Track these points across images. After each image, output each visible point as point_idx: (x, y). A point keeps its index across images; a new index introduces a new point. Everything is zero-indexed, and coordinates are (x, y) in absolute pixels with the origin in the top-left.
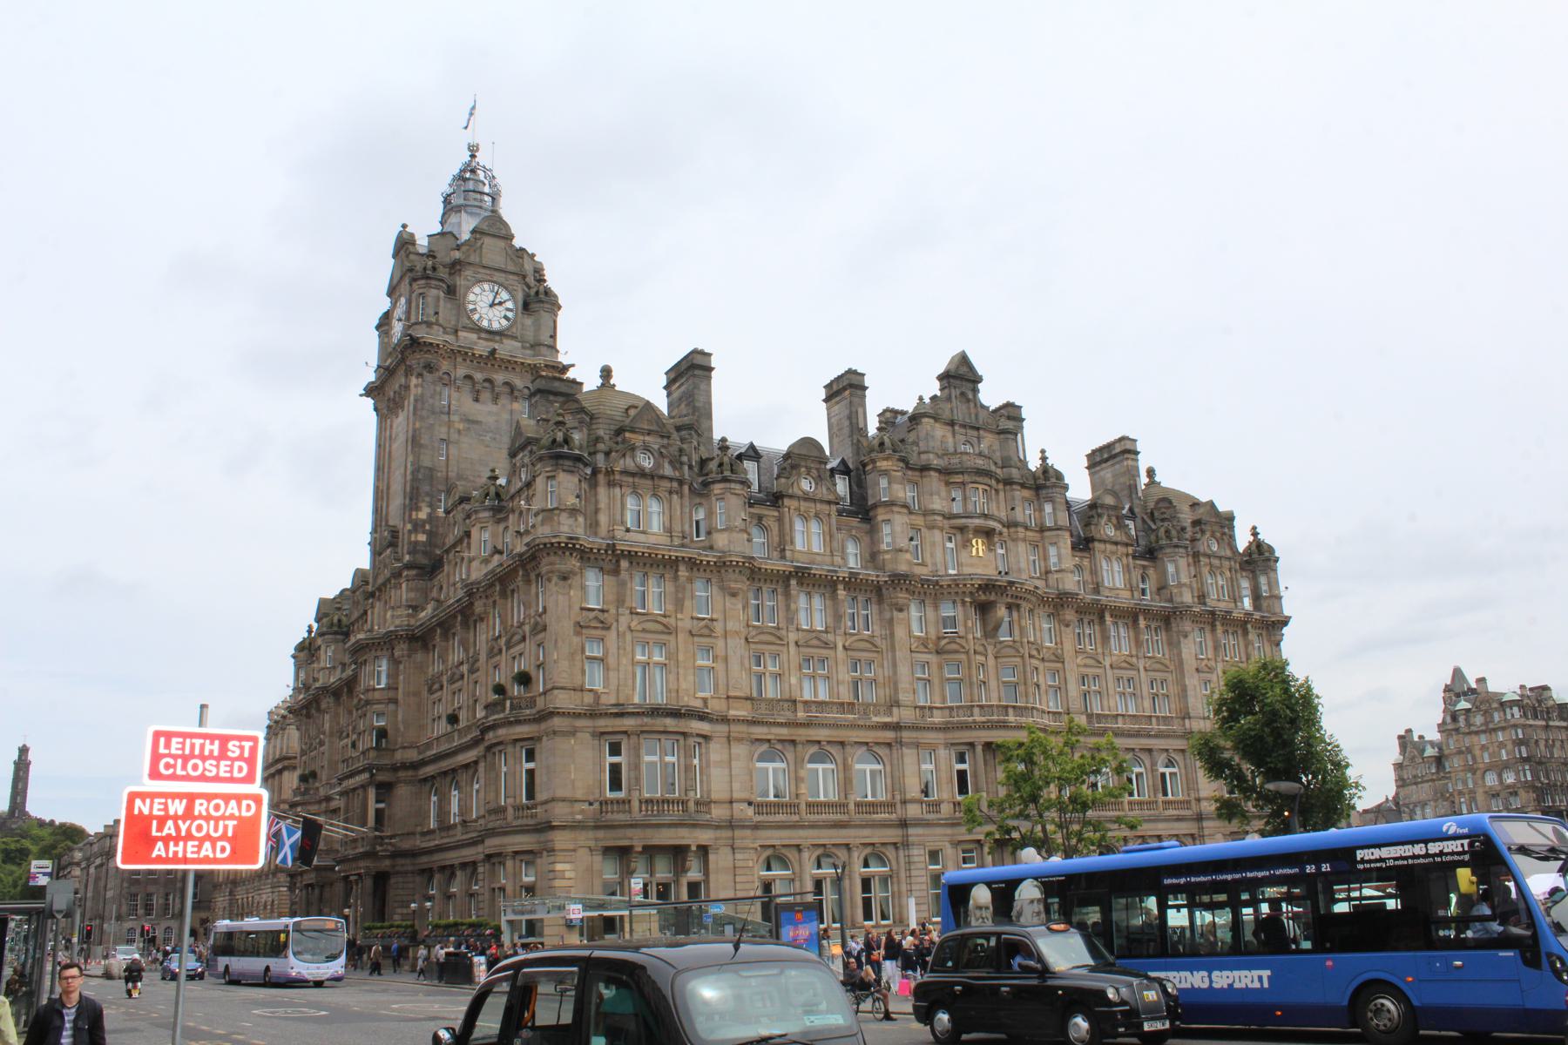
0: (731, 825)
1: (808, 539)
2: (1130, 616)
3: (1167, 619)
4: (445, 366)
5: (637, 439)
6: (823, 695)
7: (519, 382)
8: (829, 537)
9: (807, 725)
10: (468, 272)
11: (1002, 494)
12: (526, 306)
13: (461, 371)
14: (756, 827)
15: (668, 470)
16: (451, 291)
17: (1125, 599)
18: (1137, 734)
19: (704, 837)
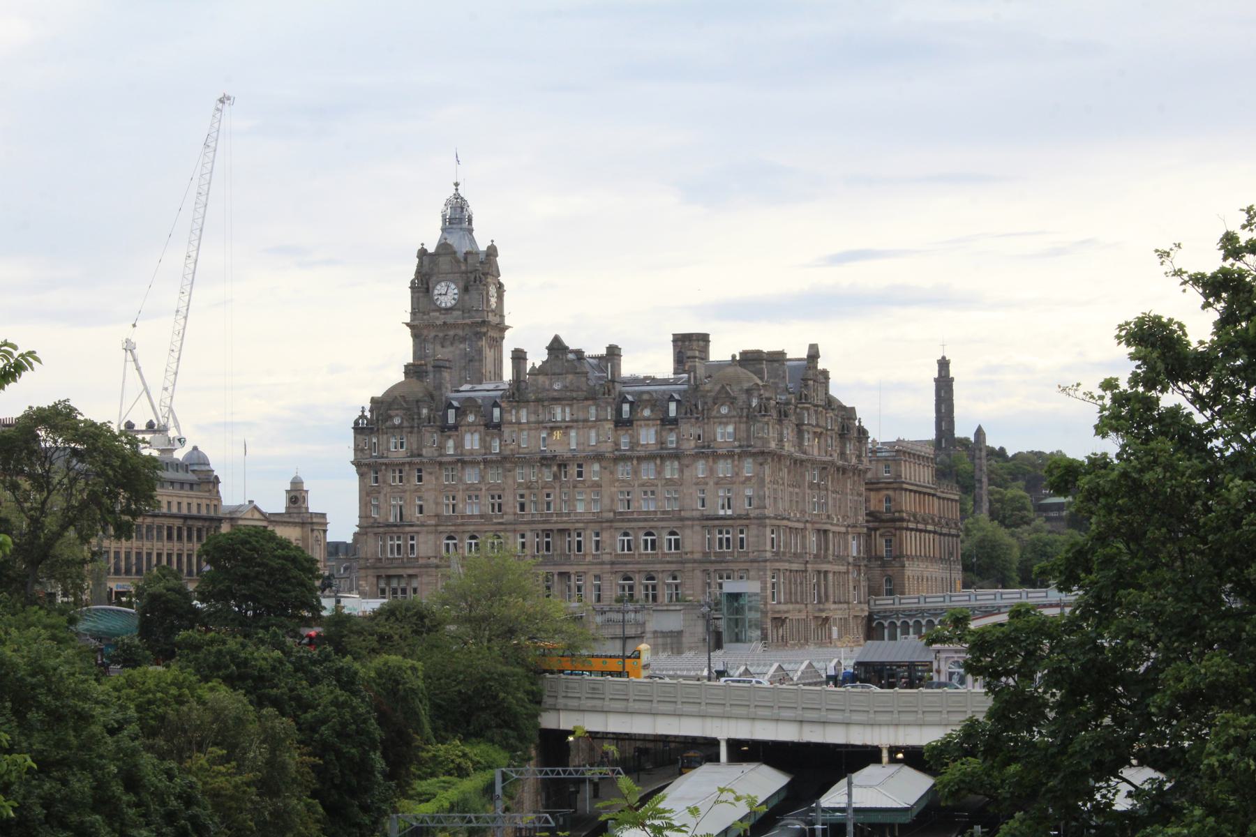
0: (427, 566)
2: (651, 457)
3: (676, 456)
4: (425, 332)
5: (392, 413)
6: (476, 512)
7: (460, 333)
8: (482, 440)
9: (463, 524)
10: (434, 279)
11: (575, 406)
12: (466, 289)
13: (433, 334)
14: (437, 567)
15: (405, 424)
16: (427, 290)
17: (654, 449)
18: (645, 520)
19: (410, 572)
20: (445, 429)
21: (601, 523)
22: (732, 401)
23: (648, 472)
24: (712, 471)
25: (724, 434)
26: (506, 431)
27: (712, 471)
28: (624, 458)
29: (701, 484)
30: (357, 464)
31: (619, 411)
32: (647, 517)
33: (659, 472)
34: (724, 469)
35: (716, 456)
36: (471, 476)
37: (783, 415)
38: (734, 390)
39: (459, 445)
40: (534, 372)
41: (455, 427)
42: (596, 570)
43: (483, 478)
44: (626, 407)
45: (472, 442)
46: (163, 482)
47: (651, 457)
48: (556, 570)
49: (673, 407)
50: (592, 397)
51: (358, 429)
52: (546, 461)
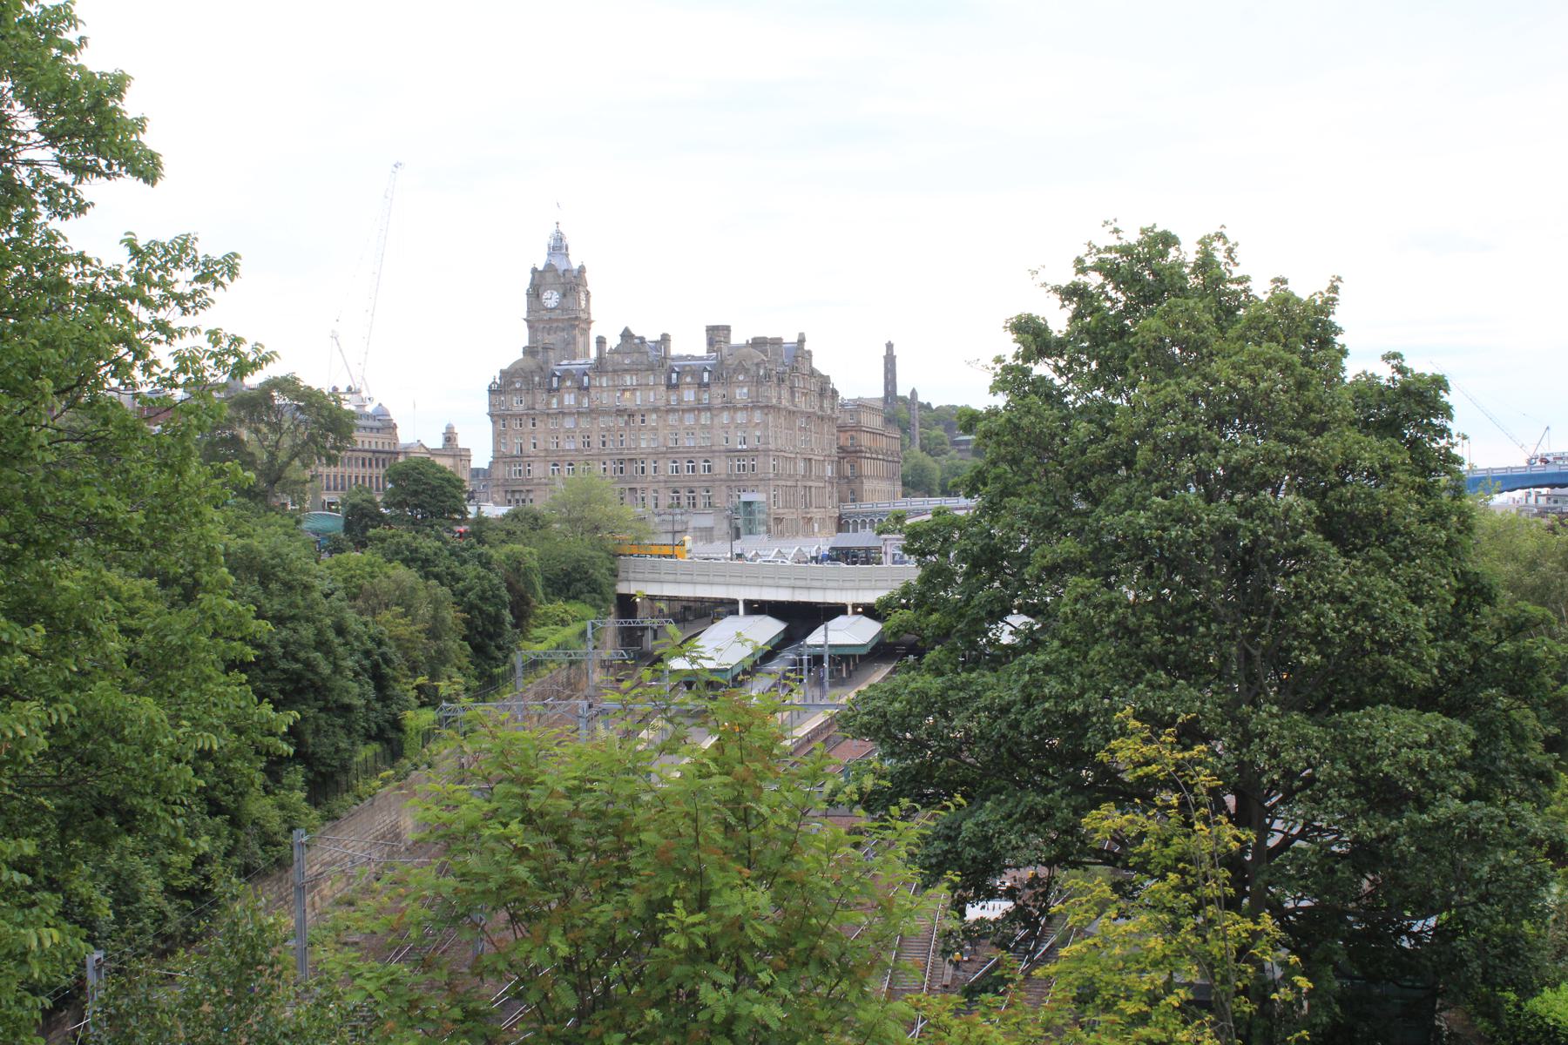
1: (569, 400)
2: (691, 410)
17: (692, 404)
20: (550, 390)
21: (657, 454)
22: (746, 371)
23: (689, 419)
24: (733, 419)
25: (741, 394)
26: (593, 392)
27: (733, 419)
28: (673, 411)
29: (725, 428)
30: (491, 415)
31: (670, 378)
32: (689, 450)
33: (697, 419)
34: (741, 417)
35: (735, 409)
36: (569, 423)
37: (781, 380)
38: (748, 364)
39: (561, 402)
40: (612, 352)
41: (558, 390)
42: (655, 486)
43: (577, 424)
44: (674, 376)
45: (569, 400)
46: (359, 428)
47: (691, 410)
48: (627, 486)
49: (706, 375)
50: (651, 368)
51: (491, 391)
52: (620, 412)
